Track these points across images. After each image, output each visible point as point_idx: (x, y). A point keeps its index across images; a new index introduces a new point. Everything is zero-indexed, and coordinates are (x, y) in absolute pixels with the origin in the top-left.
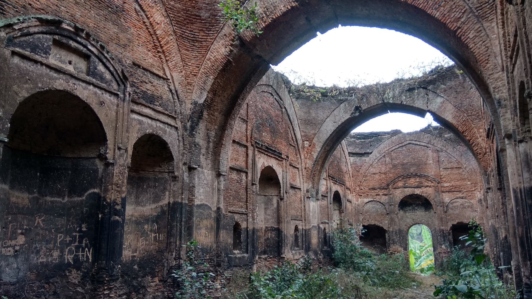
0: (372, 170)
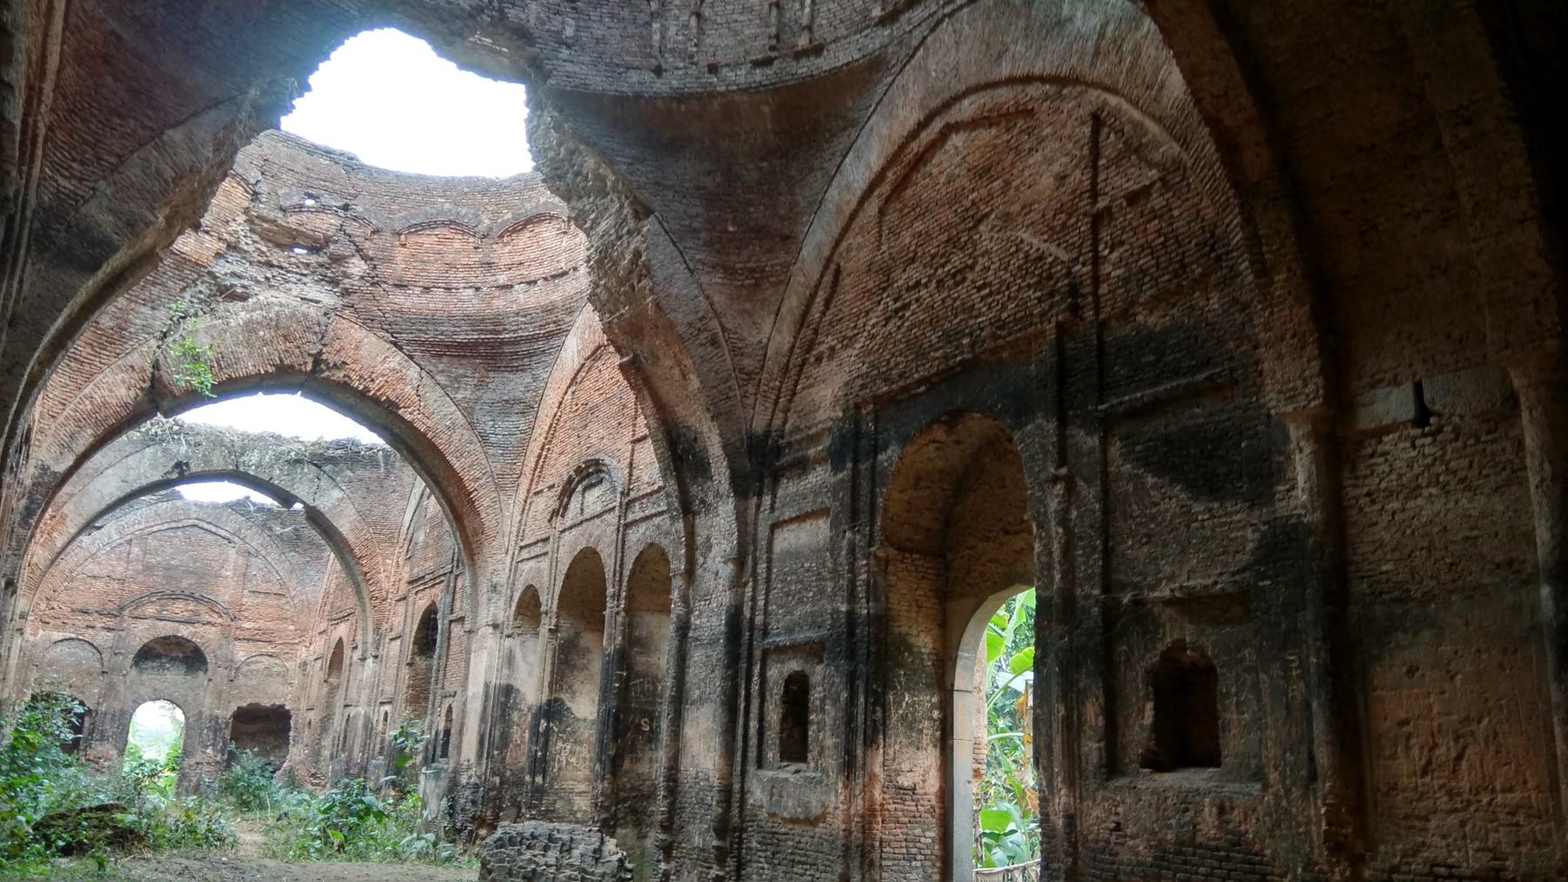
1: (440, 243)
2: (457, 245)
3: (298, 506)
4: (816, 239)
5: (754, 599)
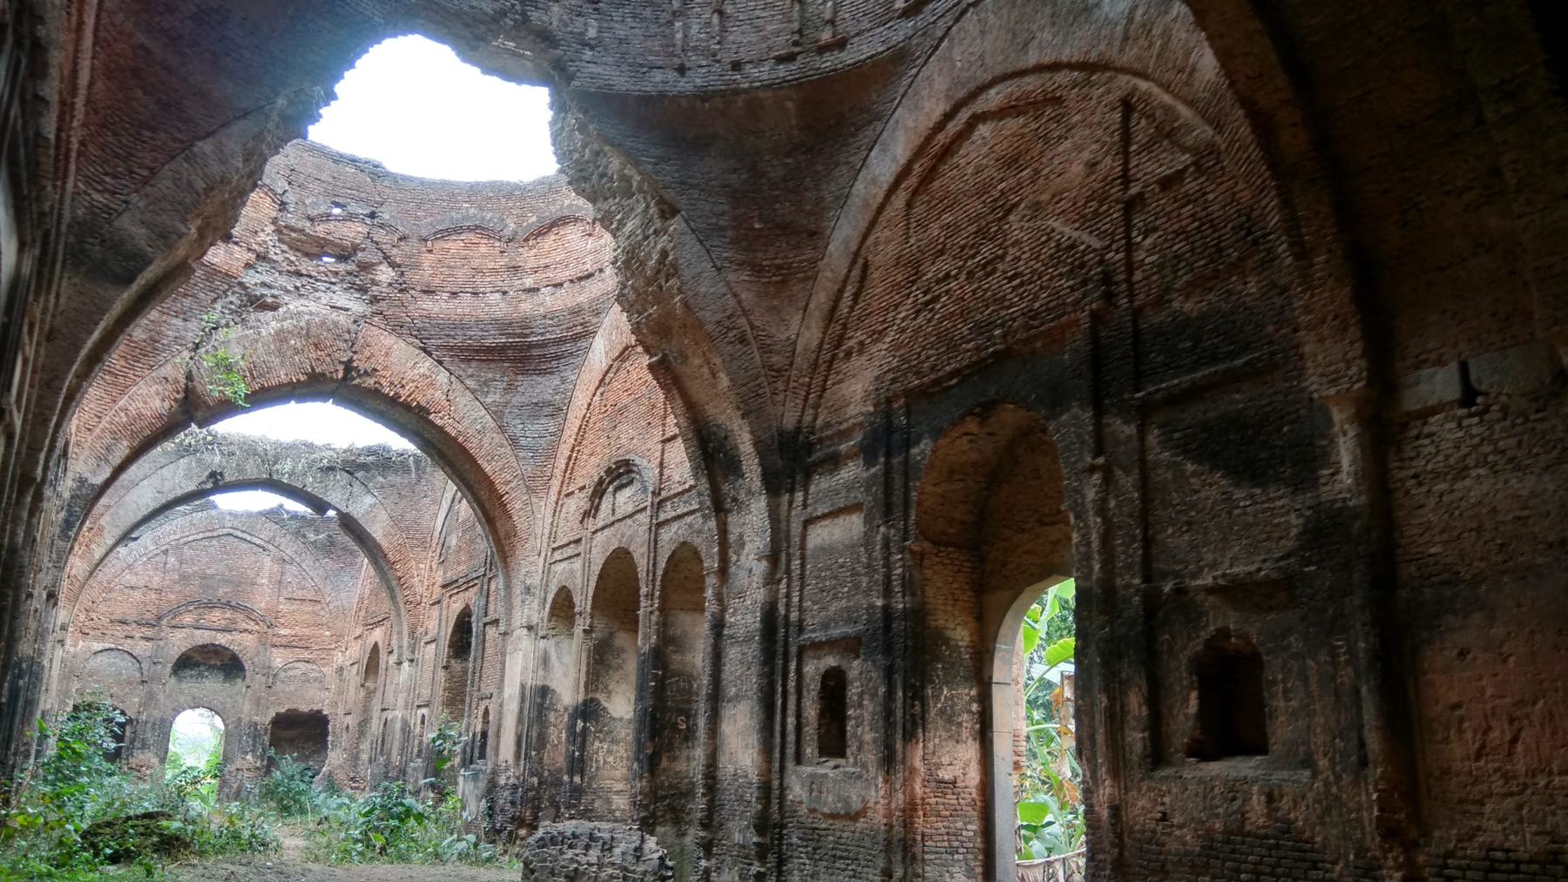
0: (128, 578)
1: (465, 248)
2: (483, 249)
3: (331, 513)
4: (843, 233)
5: (788, 596)
